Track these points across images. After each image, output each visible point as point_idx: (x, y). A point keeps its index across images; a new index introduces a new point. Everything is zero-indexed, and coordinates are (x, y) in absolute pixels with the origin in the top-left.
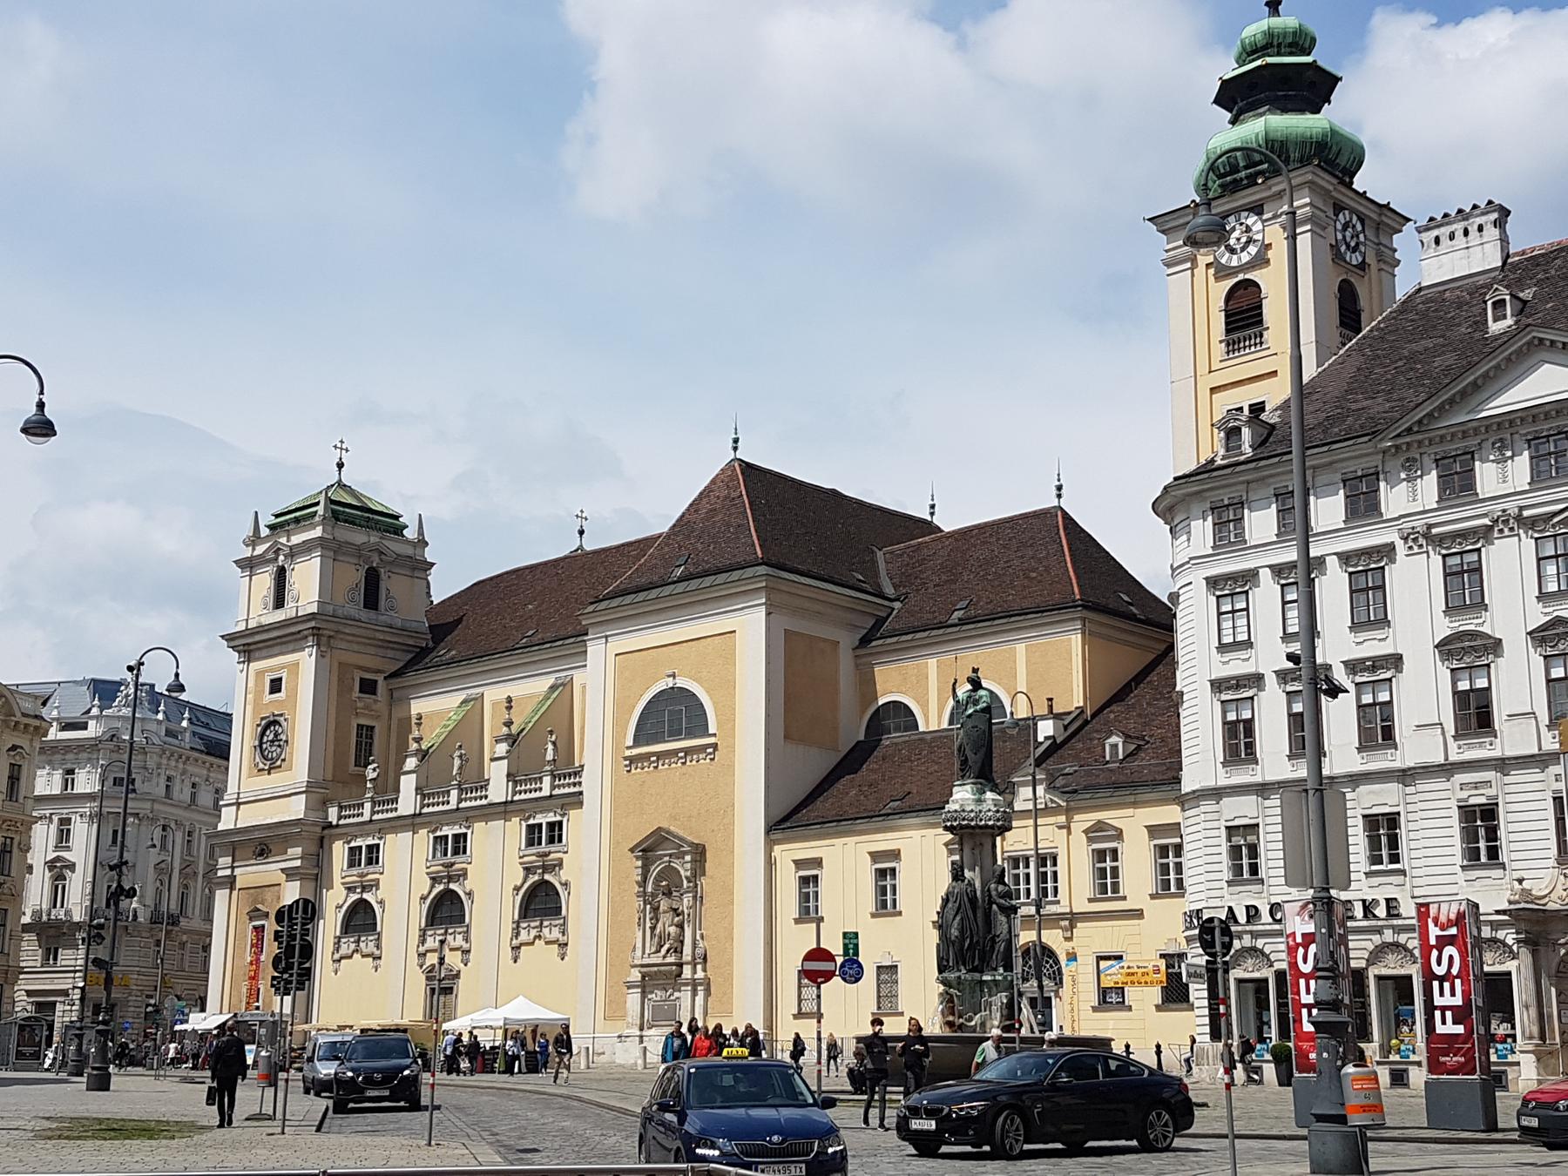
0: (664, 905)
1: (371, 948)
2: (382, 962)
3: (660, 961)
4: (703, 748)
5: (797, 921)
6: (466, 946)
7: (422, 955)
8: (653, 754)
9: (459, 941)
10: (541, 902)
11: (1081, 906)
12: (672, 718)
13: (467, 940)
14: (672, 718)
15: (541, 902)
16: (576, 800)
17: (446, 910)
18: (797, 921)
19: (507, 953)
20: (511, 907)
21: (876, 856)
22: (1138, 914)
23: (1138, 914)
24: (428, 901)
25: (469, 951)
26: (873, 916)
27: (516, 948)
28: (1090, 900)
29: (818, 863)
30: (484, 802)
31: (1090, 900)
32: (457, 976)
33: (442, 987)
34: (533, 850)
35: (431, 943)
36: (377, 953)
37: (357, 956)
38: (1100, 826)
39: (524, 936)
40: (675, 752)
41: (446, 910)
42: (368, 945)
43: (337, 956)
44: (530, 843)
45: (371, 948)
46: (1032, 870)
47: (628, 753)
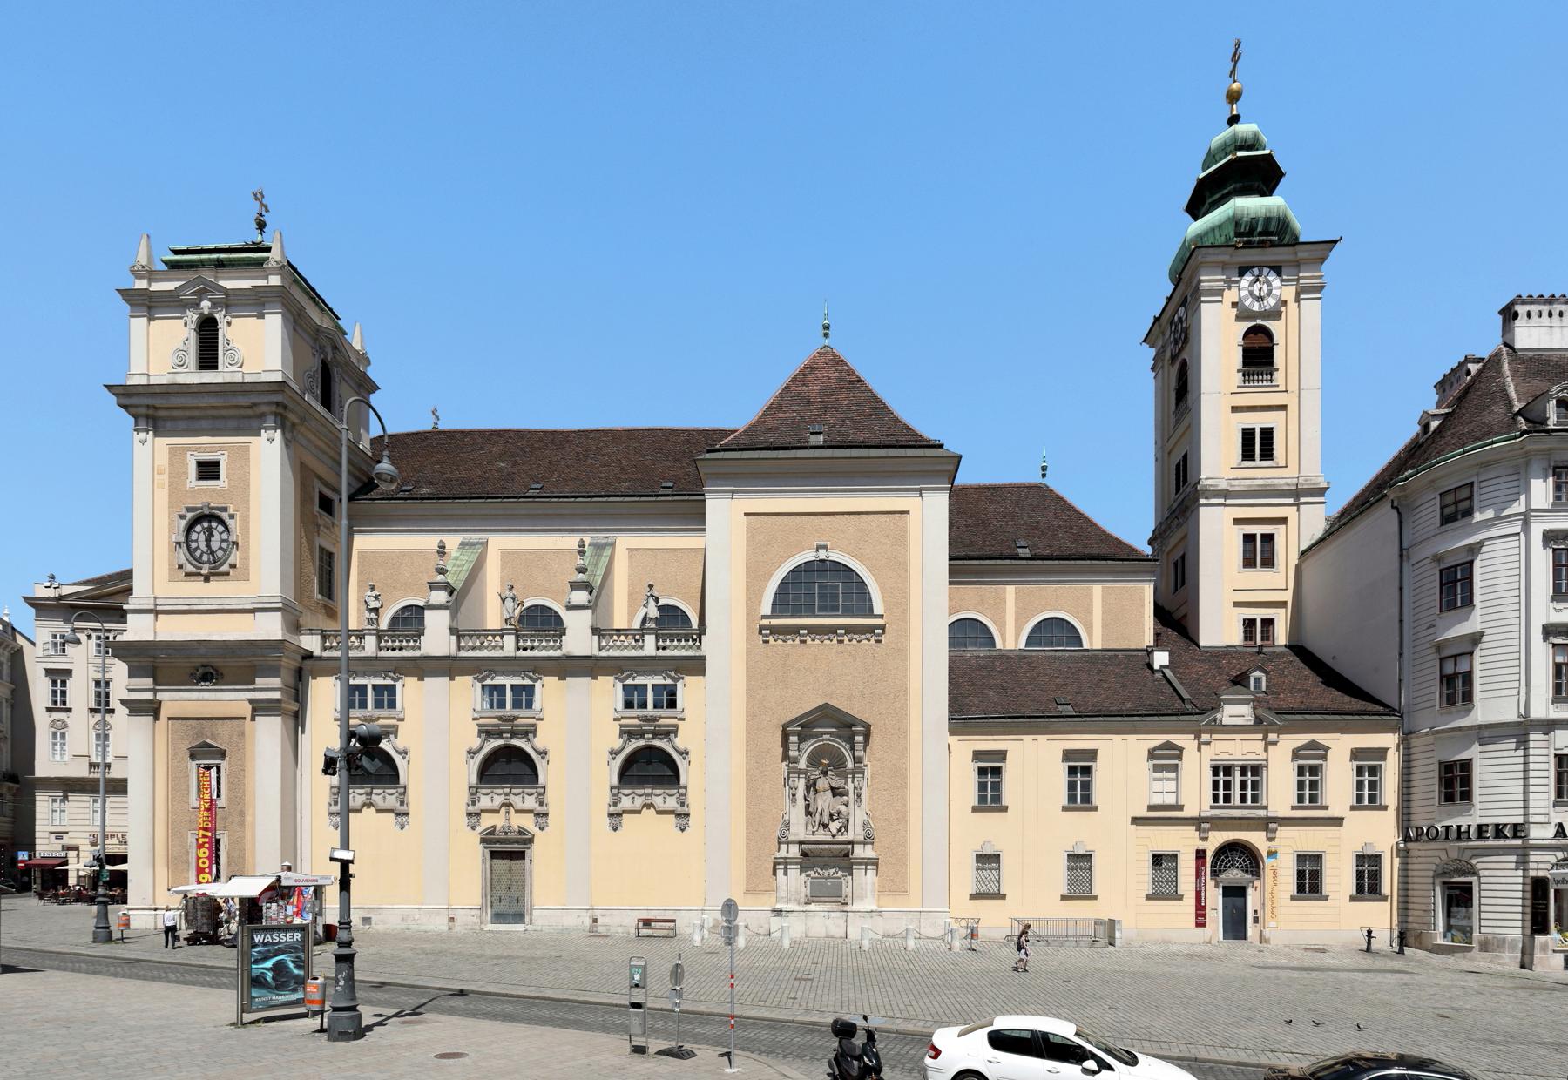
0: (822, 783)
2: (411, 819)
3: (829, 839)
4: (870, 630)
5: (975, 809)
6: (539, 809)
8: (803, 627)
10: (649, 767)
11: (1286, 812)
12: (821, 594)
14: (821, 594)
15: (649, 767)
16: (697, 666)
17: (508, 765)
18: (975, 809)
20: (610, 773)
21: (1068, 755)
22: (1337, 821)
23: (1337, 821)
24: (480, 757)
25: (546, 815)
26: (1065, 809)
27: (615, 817)
28: (1293, 808)
29: (1002, 755)
30: (558, 653)
31: (1293, 808)
32: (531, 841)
34: (636, 712)
38: (1313, 745)
39: (626, 803)
40: (832, 630)
41: (508, 765)
44: (628, 704)
46: (1237, 777)
47: (765, 622)
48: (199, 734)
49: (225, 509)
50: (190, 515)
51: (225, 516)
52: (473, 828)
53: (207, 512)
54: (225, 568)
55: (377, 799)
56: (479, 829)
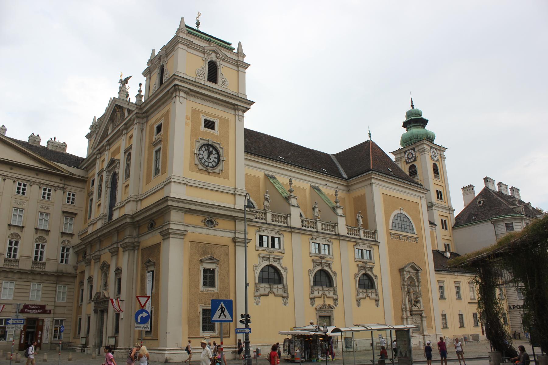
1: (281, 292)
2: (290, 300)
6: (335, 297)
7: (312, 300)
9: (331, 294)
10: (367, 282)
13: (335, 294)
17: (323, 278)
19: (355, 302)
27: (358, 301)
33: (326, 316)
35: (316, 294)
36: (285, 295)
37: (271, 295)
41: (323, 278)
42: (277, 289)
43: (257, 294)
45: (281, 292)
48: (205, 253)
49: (219, 144)
50: (202, 142)
51: (217, 146)
52: (313, 305)
53: (210, 143)
54: (217, 170)
55: (275, 291)
56: (315, 306)
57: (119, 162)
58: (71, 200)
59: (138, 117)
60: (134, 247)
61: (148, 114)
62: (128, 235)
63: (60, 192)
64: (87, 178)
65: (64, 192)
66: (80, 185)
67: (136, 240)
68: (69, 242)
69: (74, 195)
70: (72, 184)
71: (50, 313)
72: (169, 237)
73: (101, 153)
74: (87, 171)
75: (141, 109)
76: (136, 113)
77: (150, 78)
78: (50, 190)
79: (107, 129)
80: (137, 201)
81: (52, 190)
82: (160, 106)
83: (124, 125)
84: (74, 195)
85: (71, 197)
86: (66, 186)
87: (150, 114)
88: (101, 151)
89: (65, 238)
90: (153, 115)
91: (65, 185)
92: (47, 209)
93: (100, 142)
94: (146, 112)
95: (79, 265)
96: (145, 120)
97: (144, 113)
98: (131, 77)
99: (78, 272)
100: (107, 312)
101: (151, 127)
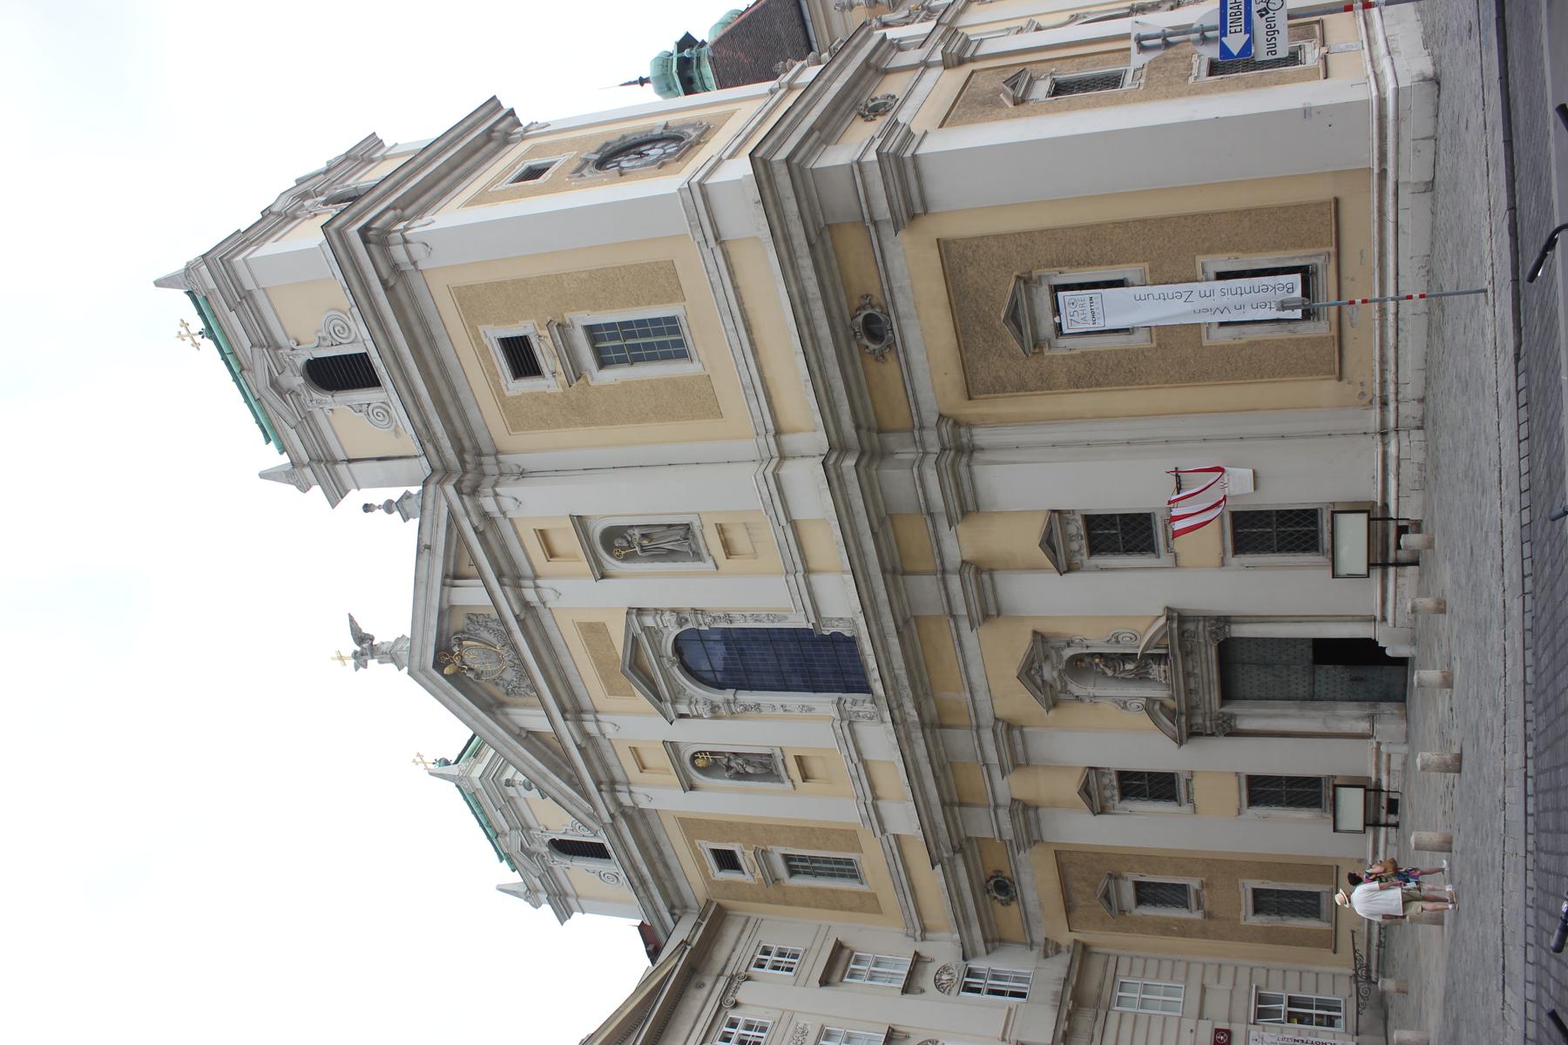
57: (640, 611)
58: (785, 961)
59: (475, 491)
60: (960, 449)
61: (467, 444)
62: (909, 478)
63: (744, 993)
64: (709, 902)
65: (748, 979)
66: (731, 932)
67: (931, 438)
68: (945, 969)
69: (766, 952)
70: (721, 954)
71: (1229, 1032)
72: (914, 156)
73: (613, 782)
74: (685, 907)
75: (447, 471)
76: (459, 492)
77: (350, 461)
78: (733, 1024)
79: (529, 738)
80: (783, 457)
81: (732, 1014)
82: (441, 363)
83: (502, 584)
84: (766, 952)
85: (772, 958)
86: (728, 972)
87: (471, 435)
88: (603, 777)
89: (927, 981)
90: (473, 415)
91: (721, 974)
92: (804, 1033)
93: (575, 782)
94: (460, 452)
95: (1039, 937)
96: (488, 461)
97: (463, 462)
98: (351, 619)
99: (1066, 938)
100: (1225, 620)
101: (517, 416)
